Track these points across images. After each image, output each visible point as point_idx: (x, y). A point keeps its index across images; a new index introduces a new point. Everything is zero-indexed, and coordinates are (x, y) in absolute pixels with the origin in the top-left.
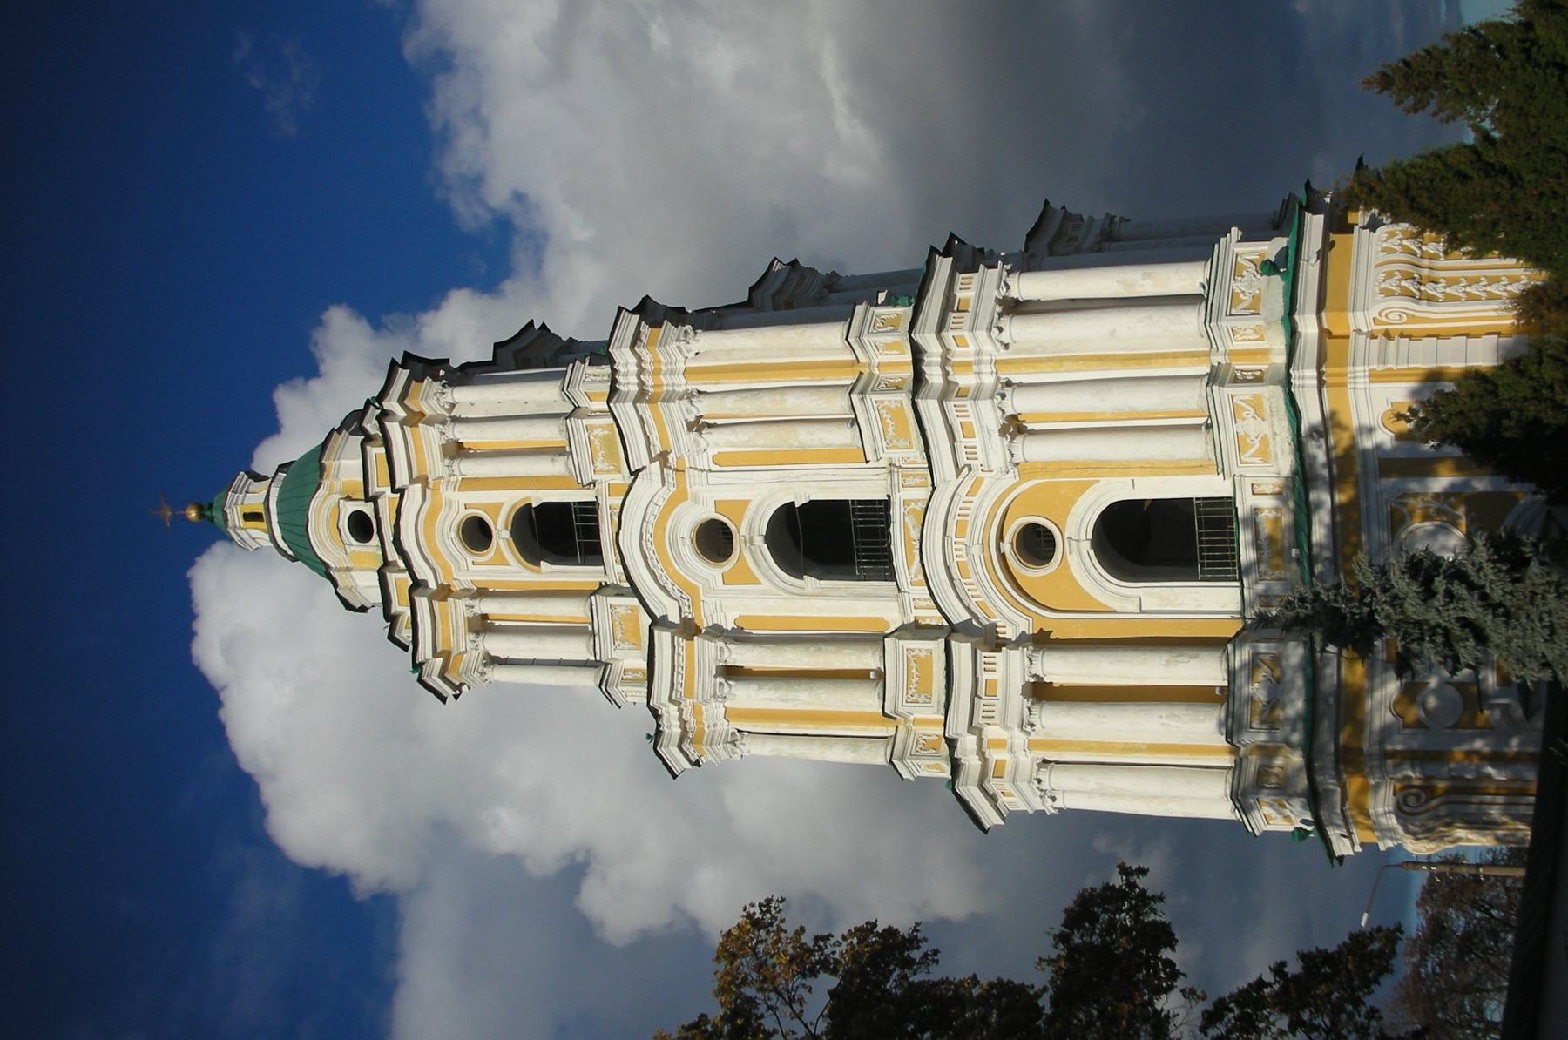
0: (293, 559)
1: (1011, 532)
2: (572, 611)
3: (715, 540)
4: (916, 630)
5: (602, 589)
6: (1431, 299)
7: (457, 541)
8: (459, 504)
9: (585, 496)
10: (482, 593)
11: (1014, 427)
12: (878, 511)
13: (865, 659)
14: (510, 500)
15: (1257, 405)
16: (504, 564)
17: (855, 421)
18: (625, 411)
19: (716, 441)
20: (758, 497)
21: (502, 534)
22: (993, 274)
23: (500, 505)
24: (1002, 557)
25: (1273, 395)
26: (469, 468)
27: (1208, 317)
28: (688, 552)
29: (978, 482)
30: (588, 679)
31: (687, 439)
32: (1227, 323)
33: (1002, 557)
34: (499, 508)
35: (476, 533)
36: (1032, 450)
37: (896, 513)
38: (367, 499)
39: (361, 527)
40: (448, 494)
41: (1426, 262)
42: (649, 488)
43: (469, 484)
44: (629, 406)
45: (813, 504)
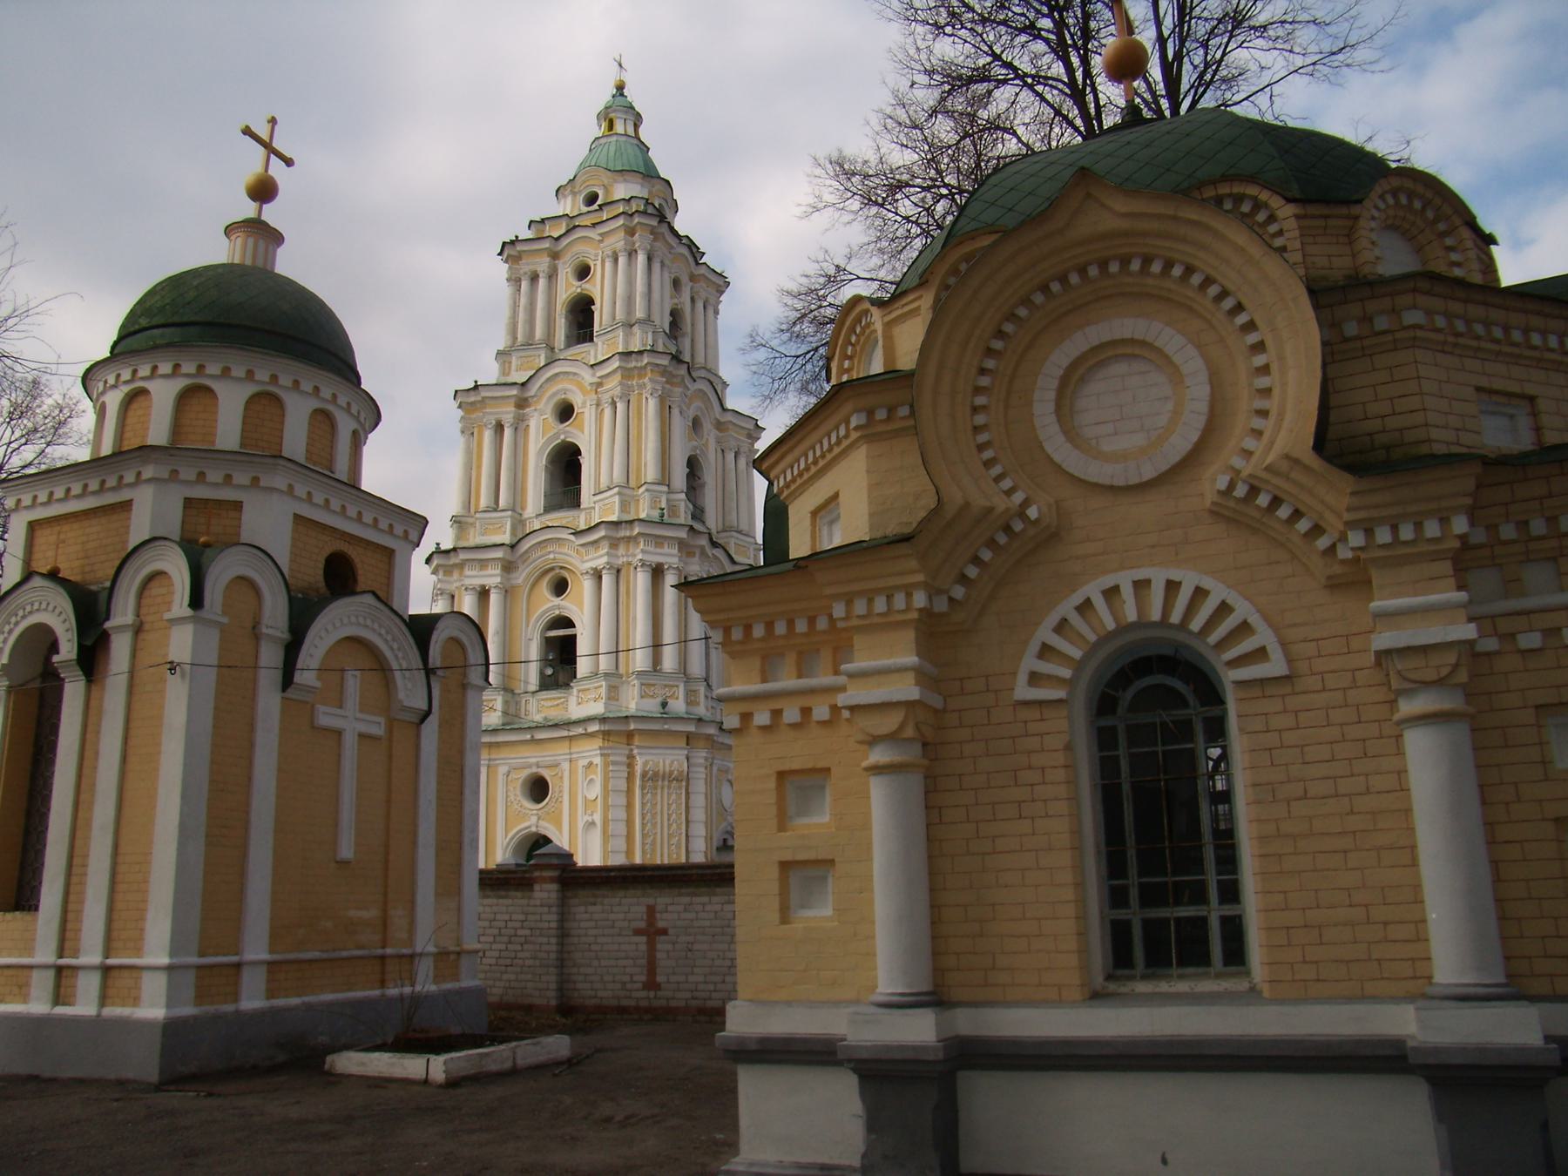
2: (539, 333)
3: (566, 412)
6: (643, 788)
10: (552, 276)
11: (597, 575)
16: (568, 288)
19: (608, 412)
20: (583, 435)
22: (675, 560)
25: (597, 708)
26: (608, 265)
27: (640, 674)
31: (606, 398)
33: (552, 569)
34: (593, 287)
36: (587, 585)
39: (591, 199)
42: (588, 377)
43: (603, 262)
44: (617, 364)
45: (580, 466)
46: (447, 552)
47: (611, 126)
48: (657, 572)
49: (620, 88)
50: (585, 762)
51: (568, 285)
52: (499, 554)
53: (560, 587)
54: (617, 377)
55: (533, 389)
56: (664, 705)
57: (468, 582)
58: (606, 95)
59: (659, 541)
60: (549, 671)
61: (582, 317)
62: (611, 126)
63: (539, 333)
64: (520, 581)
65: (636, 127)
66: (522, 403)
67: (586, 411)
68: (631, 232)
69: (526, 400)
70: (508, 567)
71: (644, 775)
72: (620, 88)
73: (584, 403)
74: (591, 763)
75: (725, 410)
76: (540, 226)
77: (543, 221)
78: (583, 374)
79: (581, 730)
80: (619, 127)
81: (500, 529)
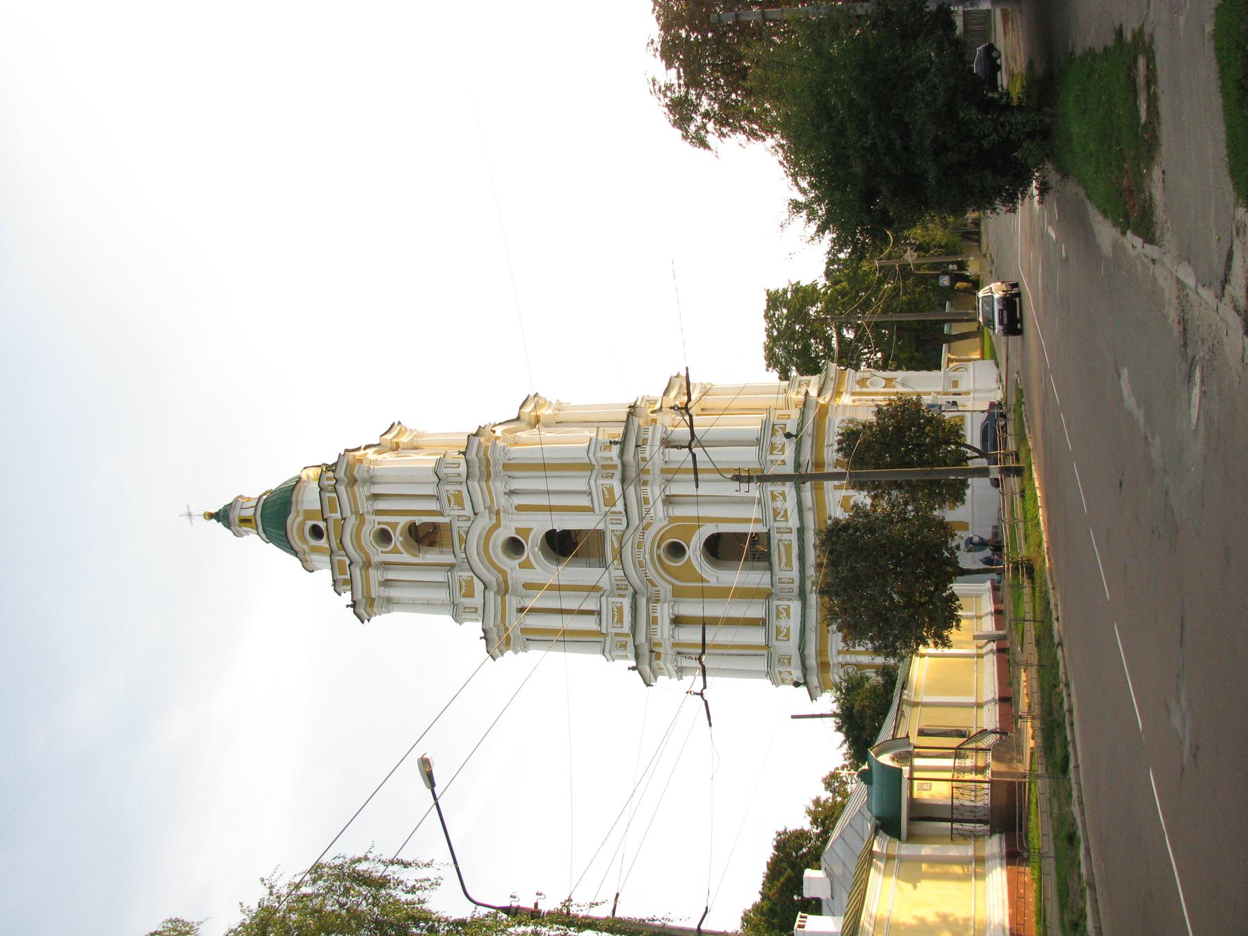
3: (515, 546)
4: (619, 590)
8: (373, 524)
10: (386, 565)
11: (669, 500)
12: (600, 535)
13: (591, 605)
14: (403, 521)
15: (783, 494)
17: (590, 493)
18: (474, 485)
19: (519, 500)
21: (397, 538)
23: (397, 524)
24: (659, 557)
29: (649, 524)
32: (770, 457)
33: (659, 557)
35: (384, 536)
37: (608, 537)
38: (325, 520)
40: (369, 518)
42: (484, 522)
43: (379, 512)
44: (476, 484)
46: (637, 657)
47: (245, 521)
51: (395, 551)
52: (642, 602)
53: (676, 550)
55: (490, 577)
56: (788, 436)
57: (666, 635)
62: (245, 521)
63: (440, 577)
64: (669, 588)
67: (514, 525)
69: (498, 585)
70: (654, 599)
72: (211, 516)
75: (518, 419)
78: (477, 532)
80: (249, 513)
81: (620, 610)
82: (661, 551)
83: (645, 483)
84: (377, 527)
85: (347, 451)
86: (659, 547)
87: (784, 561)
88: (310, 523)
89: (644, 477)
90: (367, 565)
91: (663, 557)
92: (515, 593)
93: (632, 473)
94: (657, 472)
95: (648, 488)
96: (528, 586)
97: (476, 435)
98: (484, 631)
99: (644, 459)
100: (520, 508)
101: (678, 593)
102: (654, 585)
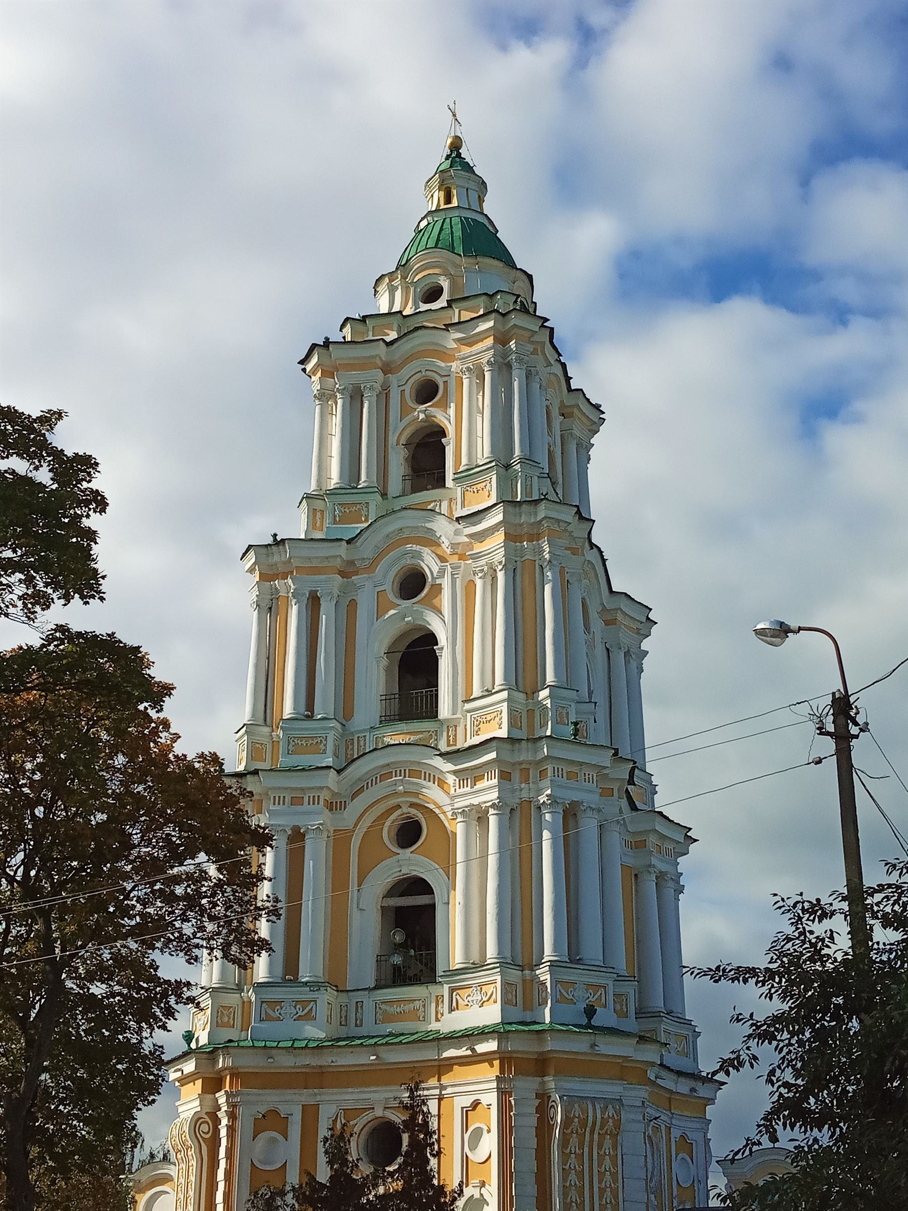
0: (418, 231)
1: (413, 811)
3: (413, 584)
5: (384, 495)
7: (418, 376)
9: (449, 483)
11: (482, 819)
12: (428, 709)
22: (596, 797)
24: (399, 807)
28: (403, 563)
30: (313, 487)
33: (399, 807)
41: (596, 1136)
48: (570, 814)
49: (456, 145)
50: (467, 1101)
51: (405, 411)
53: (409, 833)
54: (499, 538)
56: (590, 1012)
58: (438, 155)
59: (572, 771)
60: (397, 959)
61: (427, 458)
65: (481, 200)
66: (347, 571)
67: (446, 582)
68: (502, 340)
71: (567, 1122)
73: (442, 572)
74: (476, 1104)
76: (360, 327)
77: (364, 319)
79: (463, 1052)
82: (405, 809)
83: (505, 776)
84: (440, 382)
85: (552, 330)
86: (412, 805)
87: (388, 1008)
88: (445, 284)
89: (516, 776)
90: (387, 369)
91: (398, 812)
92: (344, 590)
93: (524, 755)
94: (525, 795)
95: (495, 781)
96: (353, 604)
97: (579, 513)
98: (283, 541)
99: (542, 774)
100: (470, 588)
101: (340, 841)
102: (354, 796)
